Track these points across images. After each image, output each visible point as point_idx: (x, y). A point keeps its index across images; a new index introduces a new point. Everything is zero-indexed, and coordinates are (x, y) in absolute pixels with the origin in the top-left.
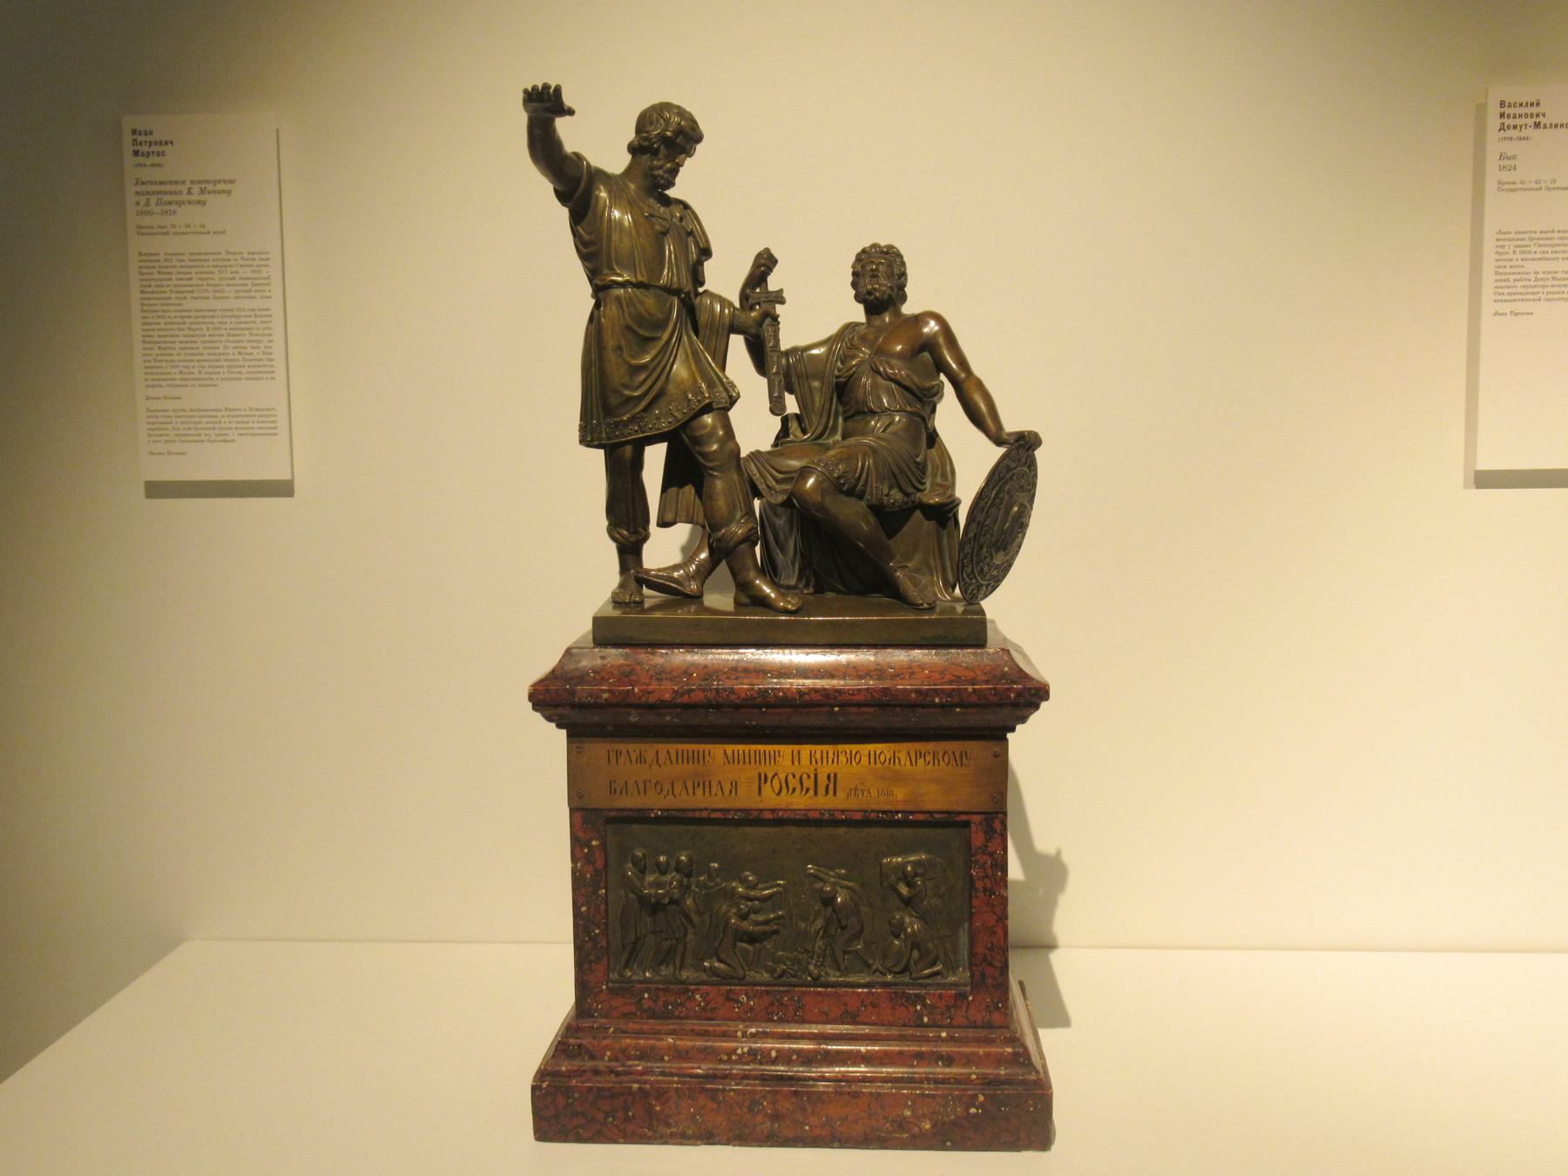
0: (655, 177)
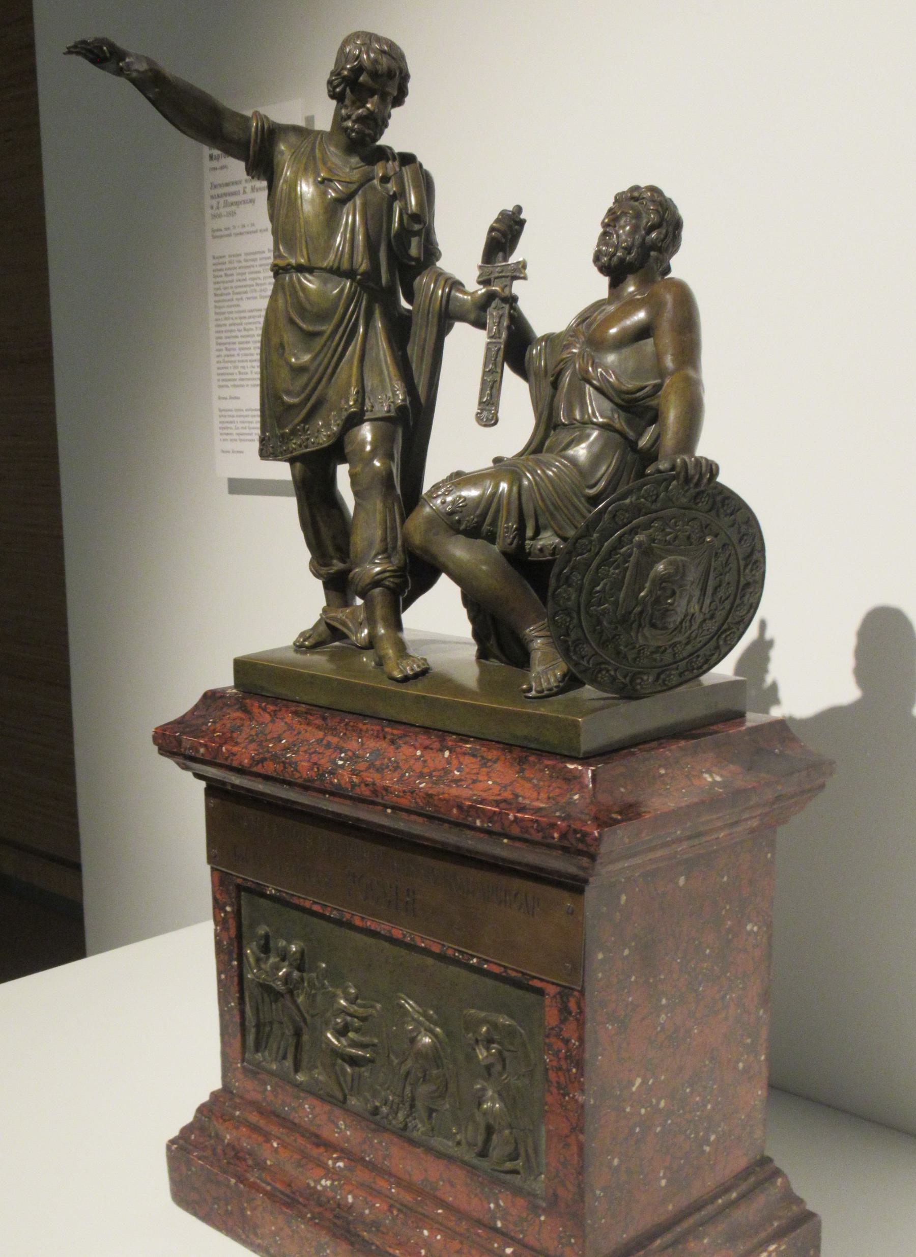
0: (346, 129)
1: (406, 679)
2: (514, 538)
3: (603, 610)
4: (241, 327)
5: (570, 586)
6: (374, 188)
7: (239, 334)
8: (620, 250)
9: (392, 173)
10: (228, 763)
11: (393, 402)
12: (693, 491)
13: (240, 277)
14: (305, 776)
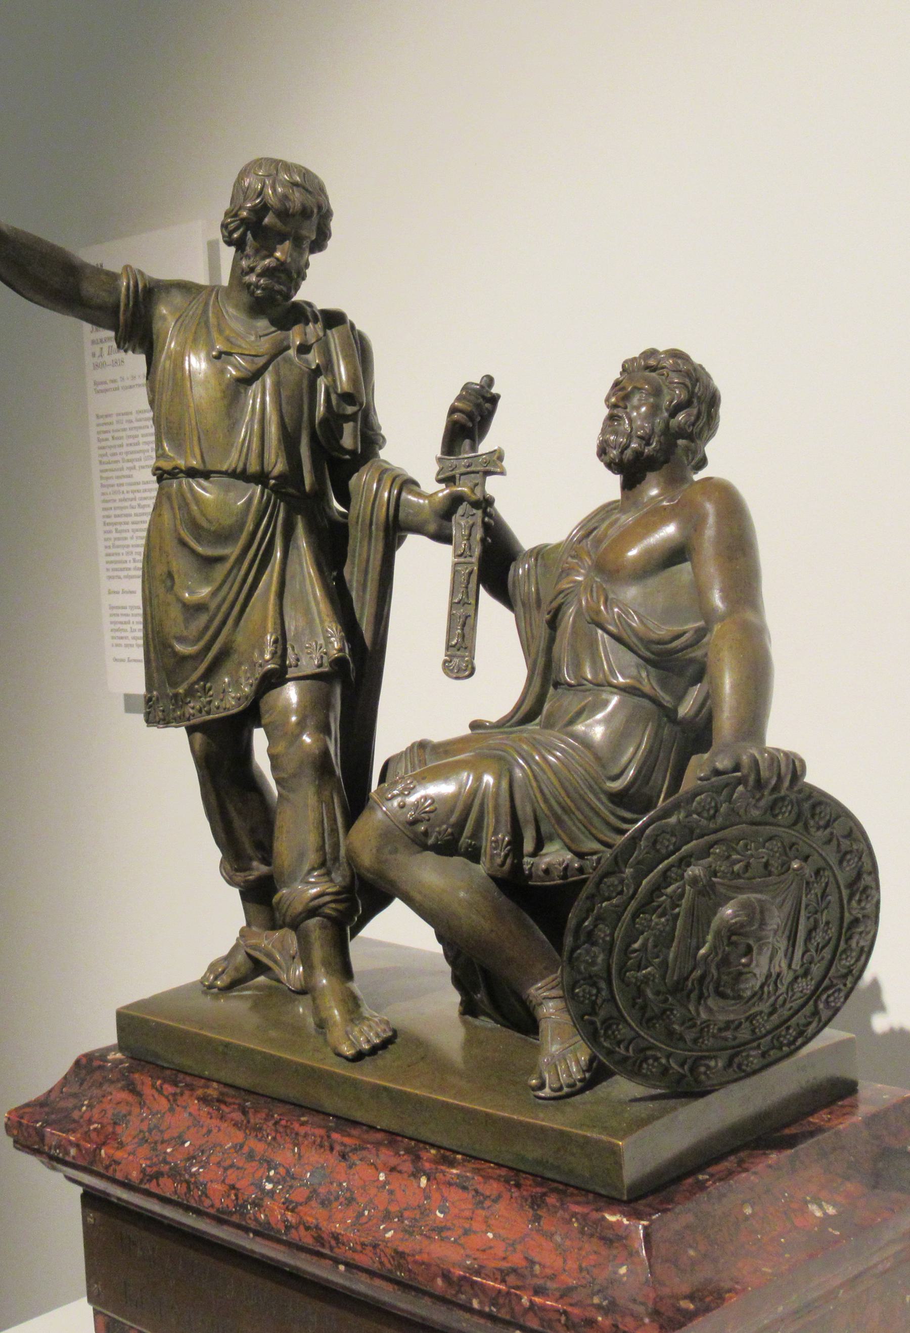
0: (248, 286)
1: (359, 1056)
2: (506, 856)
3: (644, 976)
4: (134, 503)
5: (594, 944)
6: (289, 360)
7: (133, 512)
8: (635, 440)
9: (313, 340)
10: (110, 1173)
11: (326, 653)
12: (767, 798)
13: (131, 441)
14: (218, 1205)
